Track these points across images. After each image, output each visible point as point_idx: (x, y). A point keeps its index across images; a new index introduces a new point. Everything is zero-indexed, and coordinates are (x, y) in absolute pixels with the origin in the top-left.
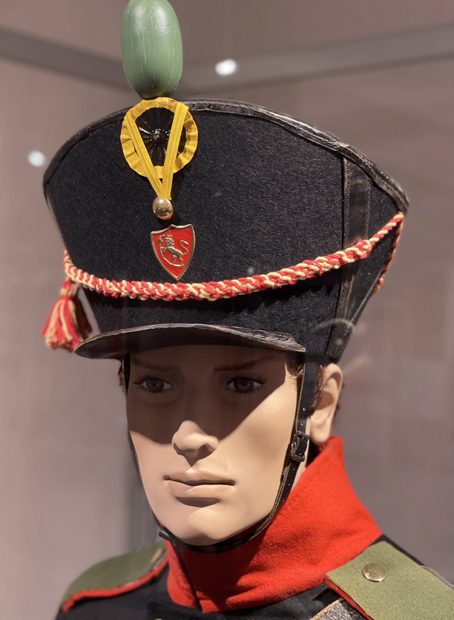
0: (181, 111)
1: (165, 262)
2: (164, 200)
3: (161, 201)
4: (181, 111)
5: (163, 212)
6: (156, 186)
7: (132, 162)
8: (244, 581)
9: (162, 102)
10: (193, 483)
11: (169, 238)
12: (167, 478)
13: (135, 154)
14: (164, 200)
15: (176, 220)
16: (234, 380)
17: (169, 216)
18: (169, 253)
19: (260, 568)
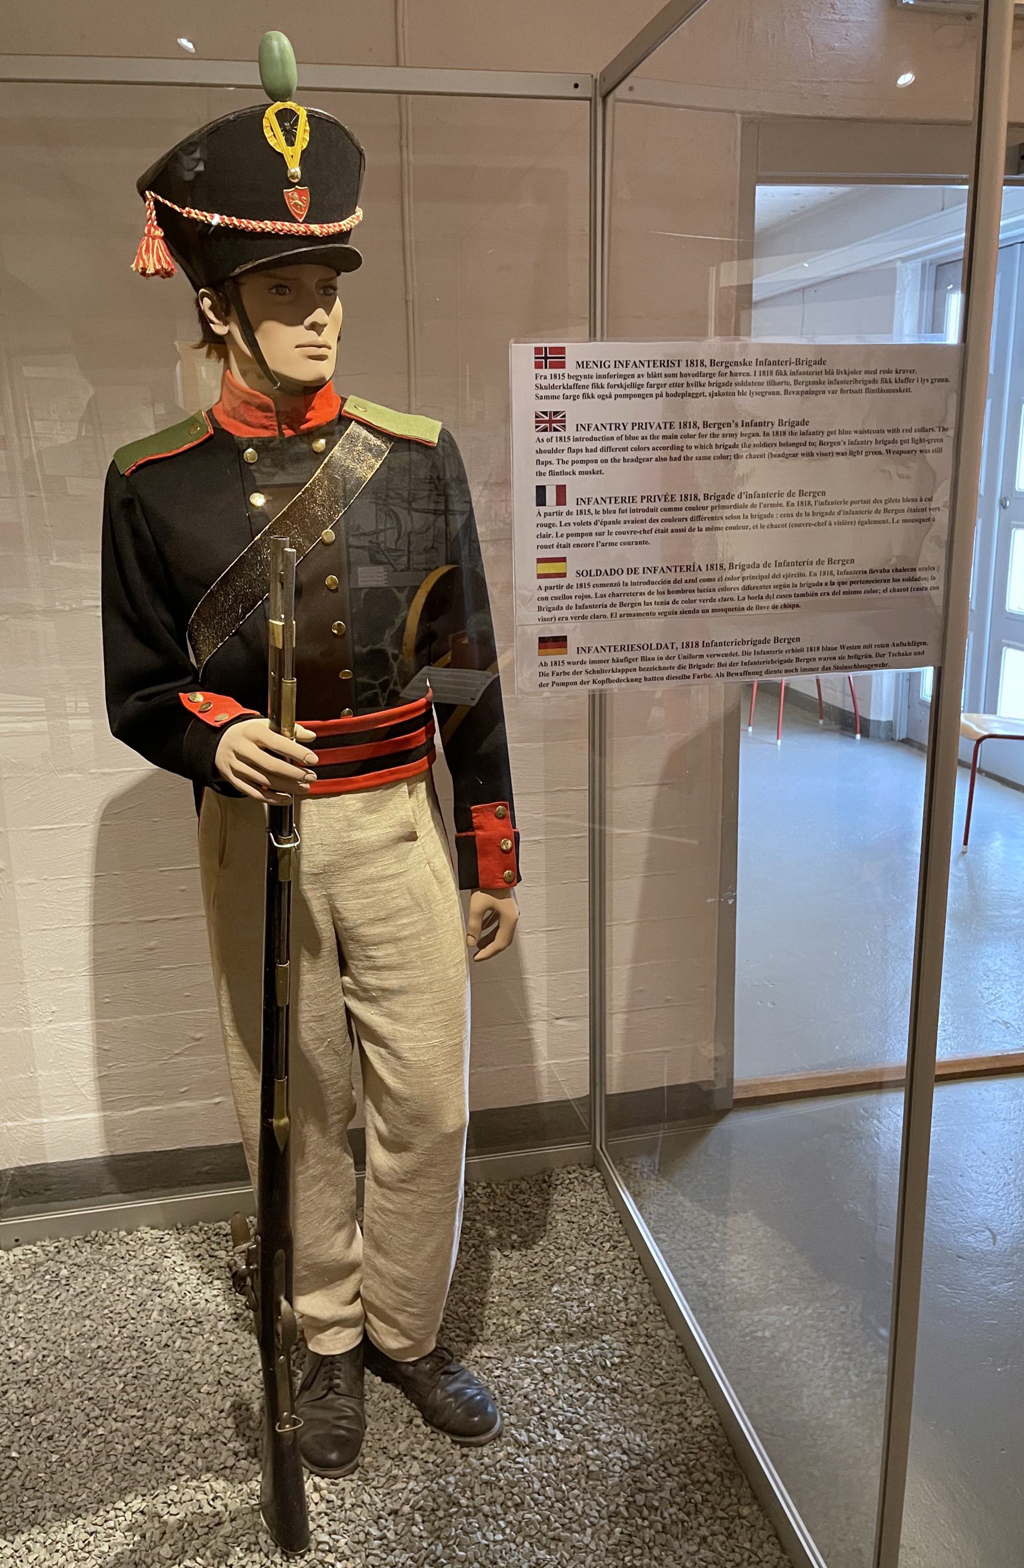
0: (302, 113)
1: (293, 211)
2: (295, 169)
3: (293, 171)
4: (302, 113)
5: (293, 177)
6: (287, 159)
7: (272, 142)
8: (308, 416)
9: (290, 104)
10: (320, 347)
11: (296, 195)
12: (297, 347)
13: (275, 138)
14: (295, 169)
15: (297, 184)
16: (324, 288)
17: (296, 181)
18: (296, 205)
19: (313, 409)
